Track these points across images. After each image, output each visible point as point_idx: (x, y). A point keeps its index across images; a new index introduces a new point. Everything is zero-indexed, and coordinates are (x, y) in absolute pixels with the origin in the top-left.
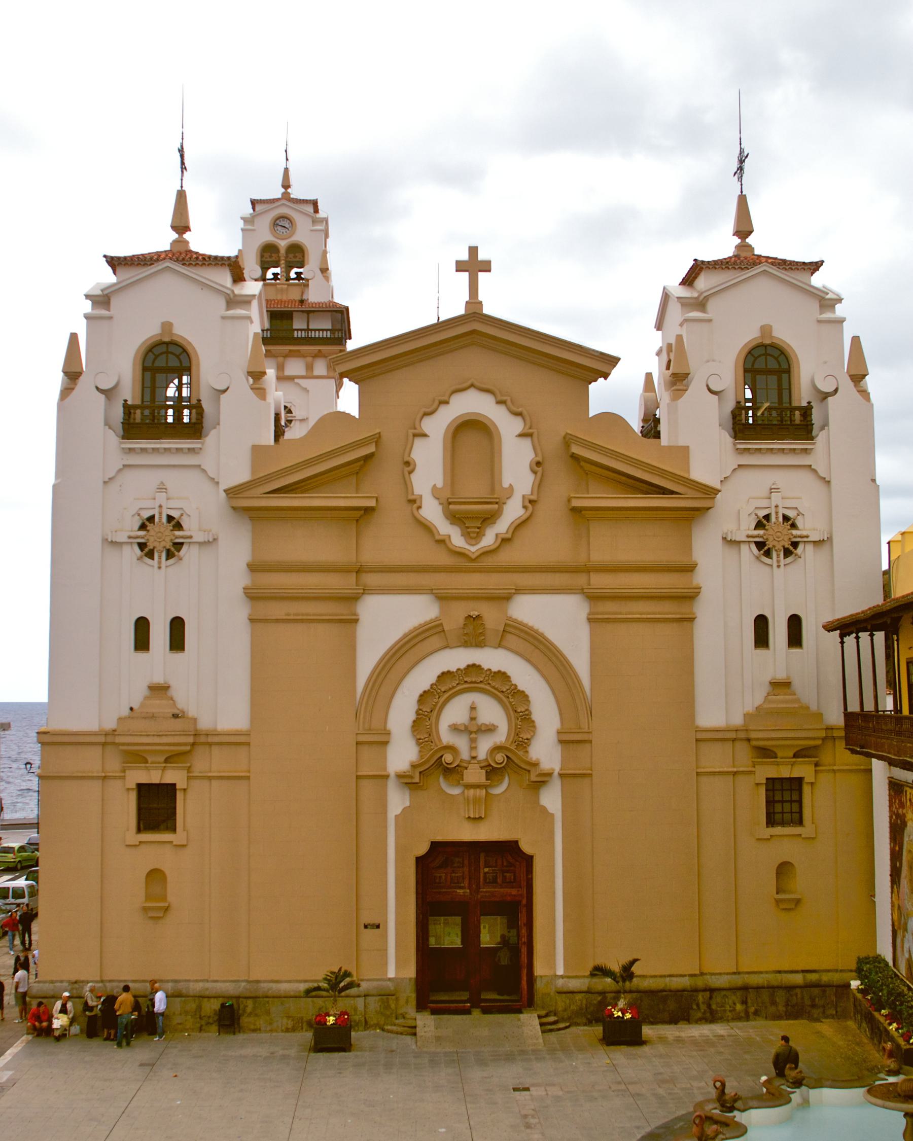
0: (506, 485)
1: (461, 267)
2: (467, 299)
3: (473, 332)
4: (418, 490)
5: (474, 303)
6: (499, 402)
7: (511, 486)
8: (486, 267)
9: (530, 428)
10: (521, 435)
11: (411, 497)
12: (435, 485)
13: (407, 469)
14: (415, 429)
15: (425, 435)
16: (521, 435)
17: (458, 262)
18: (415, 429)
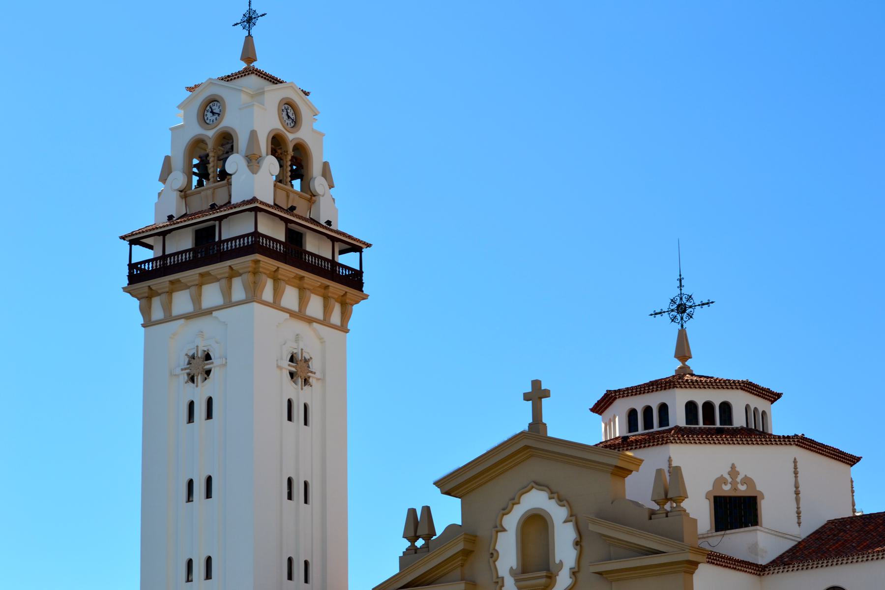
0: (557, 561)
1: (527, 397)
2: (531, 421)
3: (527, 447)
4: (500, 574)
5: (537, 425)
6: (550, 498)
7: (561, 561)
8: (546, 394)
9: (571, 516)
10: (565, 522)
11: (495, 580)
12: (512, 567)
13: (491, 560)
14: (496, 527)
15: (504, 530)
16: (565, 522)
17: (525, 394)
18: (496, 527)
